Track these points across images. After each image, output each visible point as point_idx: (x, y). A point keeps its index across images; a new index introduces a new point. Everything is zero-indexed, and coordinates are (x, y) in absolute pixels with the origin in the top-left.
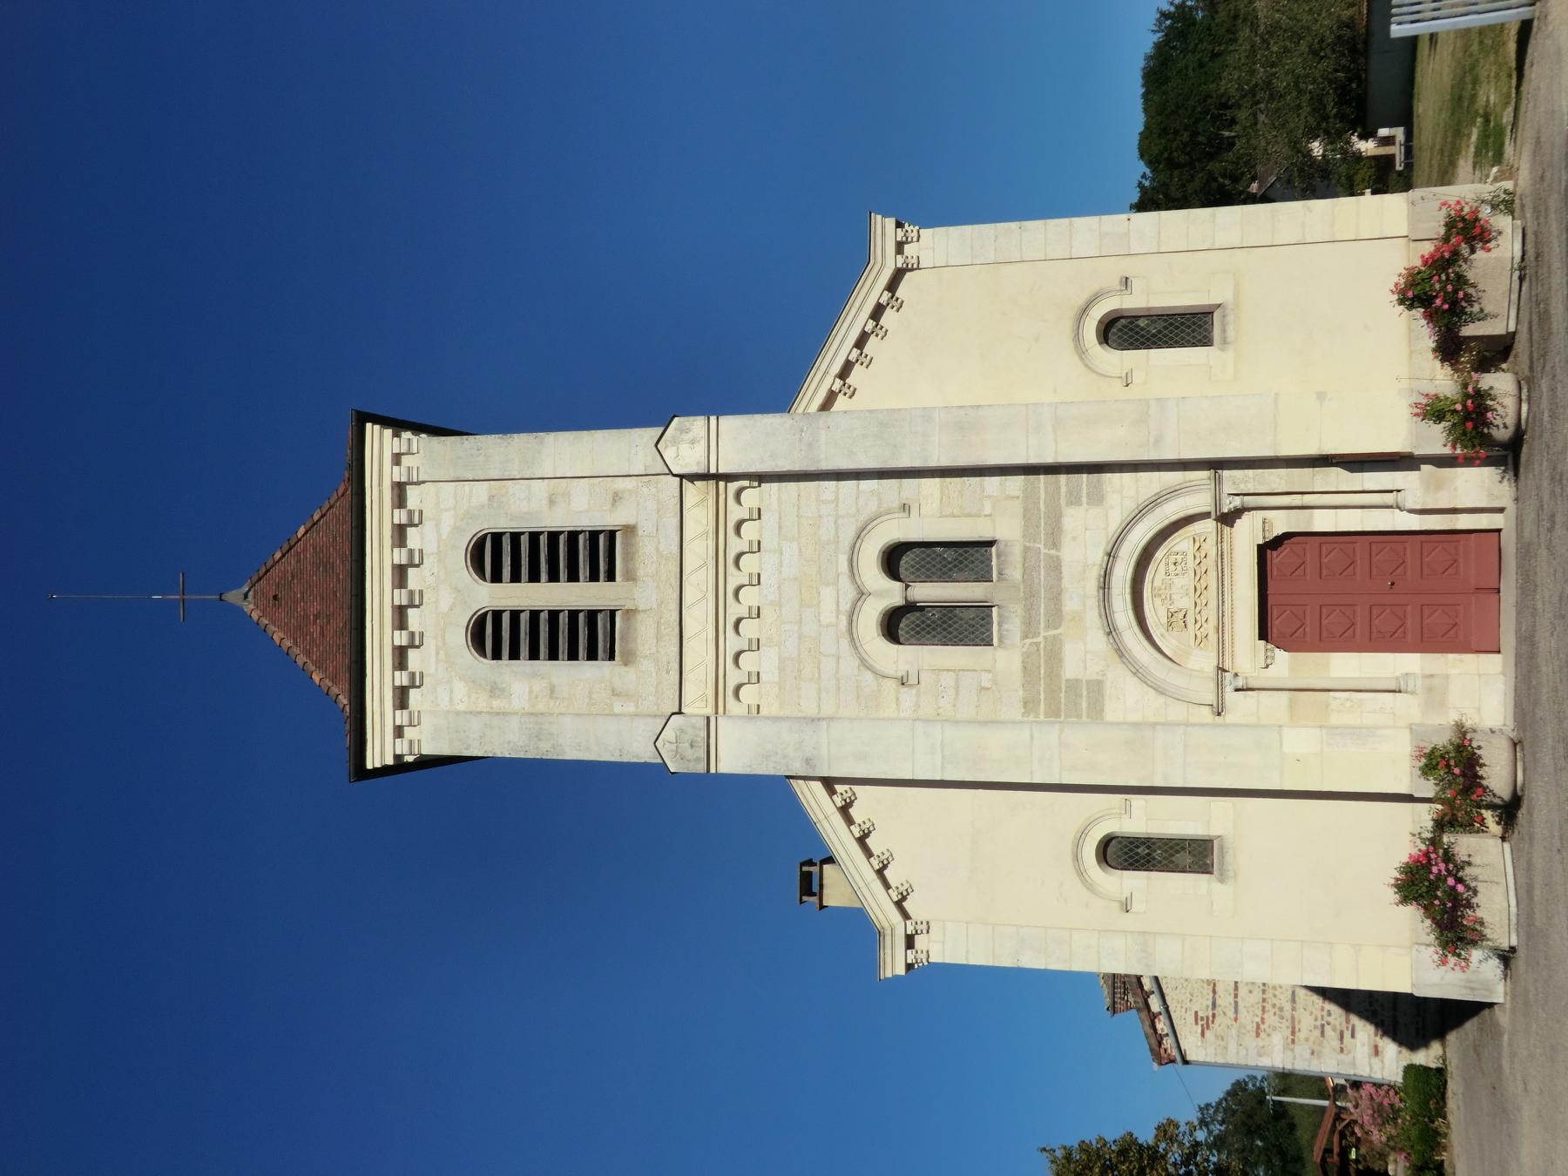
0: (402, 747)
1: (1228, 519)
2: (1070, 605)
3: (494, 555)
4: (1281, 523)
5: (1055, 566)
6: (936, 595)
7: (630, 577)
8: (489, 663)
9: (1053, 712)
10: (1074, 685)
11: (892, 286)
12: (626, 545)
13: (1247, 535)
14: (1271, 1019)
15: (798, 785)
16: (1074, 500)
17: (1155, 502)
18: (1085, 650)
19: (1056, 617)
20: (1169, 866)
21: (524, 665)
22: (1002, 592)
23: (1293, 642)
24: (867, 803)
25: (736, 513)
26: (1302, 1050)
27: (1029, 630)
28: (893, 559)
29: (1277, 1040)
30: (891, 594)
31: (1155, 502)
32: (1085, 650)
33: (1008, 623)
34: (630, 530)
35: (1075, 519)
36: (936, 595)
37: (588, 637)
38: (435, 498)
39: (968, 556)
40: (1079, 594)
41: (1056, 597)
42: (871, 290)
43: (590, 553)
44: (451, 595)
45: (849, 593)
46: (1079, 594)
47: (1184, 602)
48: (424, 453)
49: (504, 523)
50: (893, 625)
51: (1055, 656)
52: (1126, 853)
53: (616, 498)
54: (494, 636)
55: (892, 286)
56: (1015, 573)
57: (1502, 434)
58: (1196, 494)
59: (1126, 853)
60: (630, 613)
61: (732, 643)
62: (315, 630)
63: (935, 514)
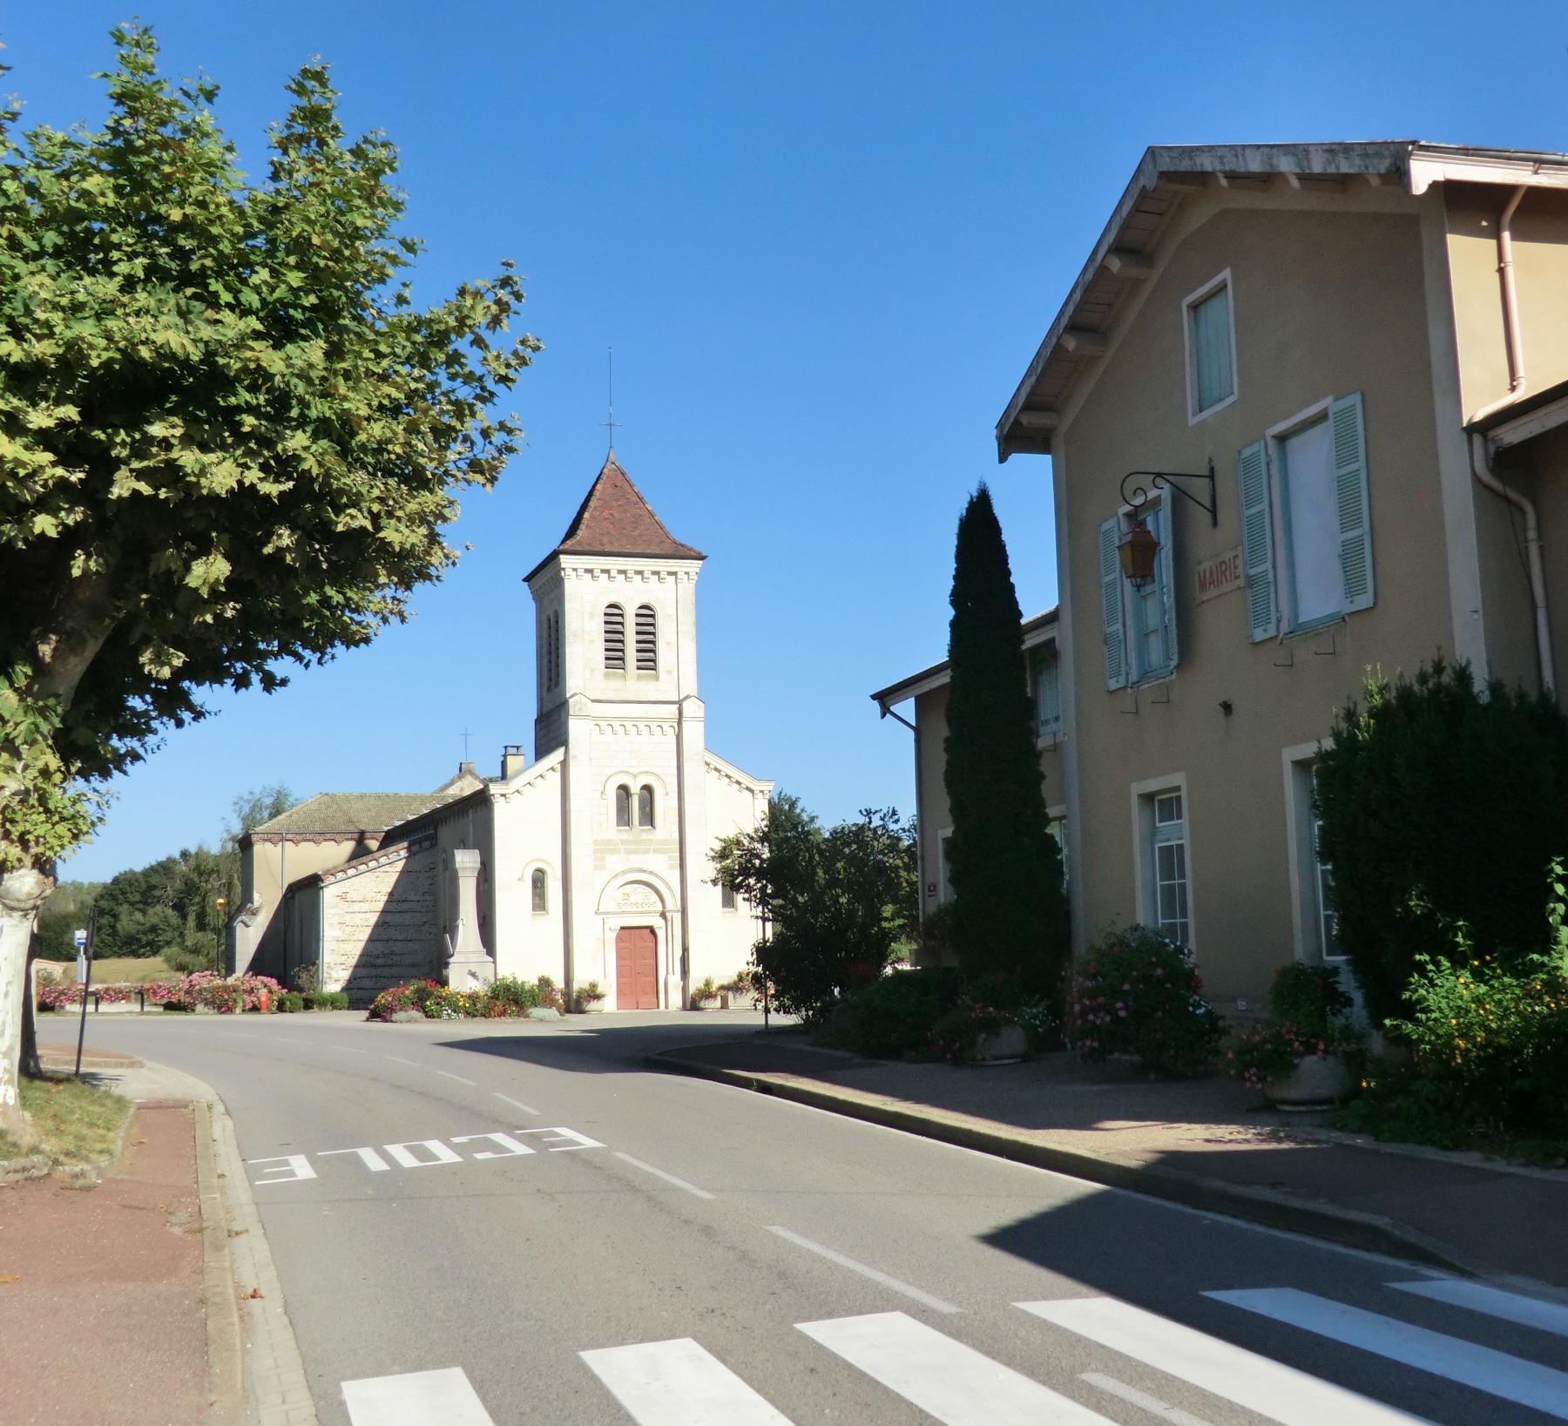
0: (568, 571)
1: (663, 915)
2: (633, 857)
3: (647, 614)
4: (661, 934)
5: (646, 852)
6: (636, 806)
7: (639, 677)
8: (603, 610)
9: (596, 851)
10: (603, 859)
11: (748, 789)
12: (647, 676)
13: (657, 923)
14: (348, 930)
15: (562, 750)
16: (670, 858)
17: (670, 889)
18: (615, 863)
19: (628, 852)
20: (534, 894)
21: (603, 627)
22: (638, 831)
23: (619, 939)
24: (556, 778)
25: (666, 726)
26: (334, 945)
27: (623, 842)
28: (647, 789)
29: (338, 933)
30: (635, 789)
31: (670, 889)
32: (615, 863)
33: (624, 834)
34: (657, 678)
35: (663, 858)
36: (636, 806)
37: (615, 657)
38: (667, 589)
39: (648, 818)
40: (637, 861)
41: (636, 852)
42: (747, 781)
43: (648, 661)
44: (631, 595)
45: (635, 771)
46: (637, 861)
47: (632, 899)
48: (687, 588)
49: (661, 621)
50: (624, 790)
51: (615, 851)
52: (539, 881)
53: (669, 672)
54: (614, 613)
55: (748, 789)
56: (644, 836)
57: (702, 1004)
58: (673, 904)
59: (539, 881)
60: (624, 677)
61: (616, 724)
62: (606, 514)
63: (665, 806)
